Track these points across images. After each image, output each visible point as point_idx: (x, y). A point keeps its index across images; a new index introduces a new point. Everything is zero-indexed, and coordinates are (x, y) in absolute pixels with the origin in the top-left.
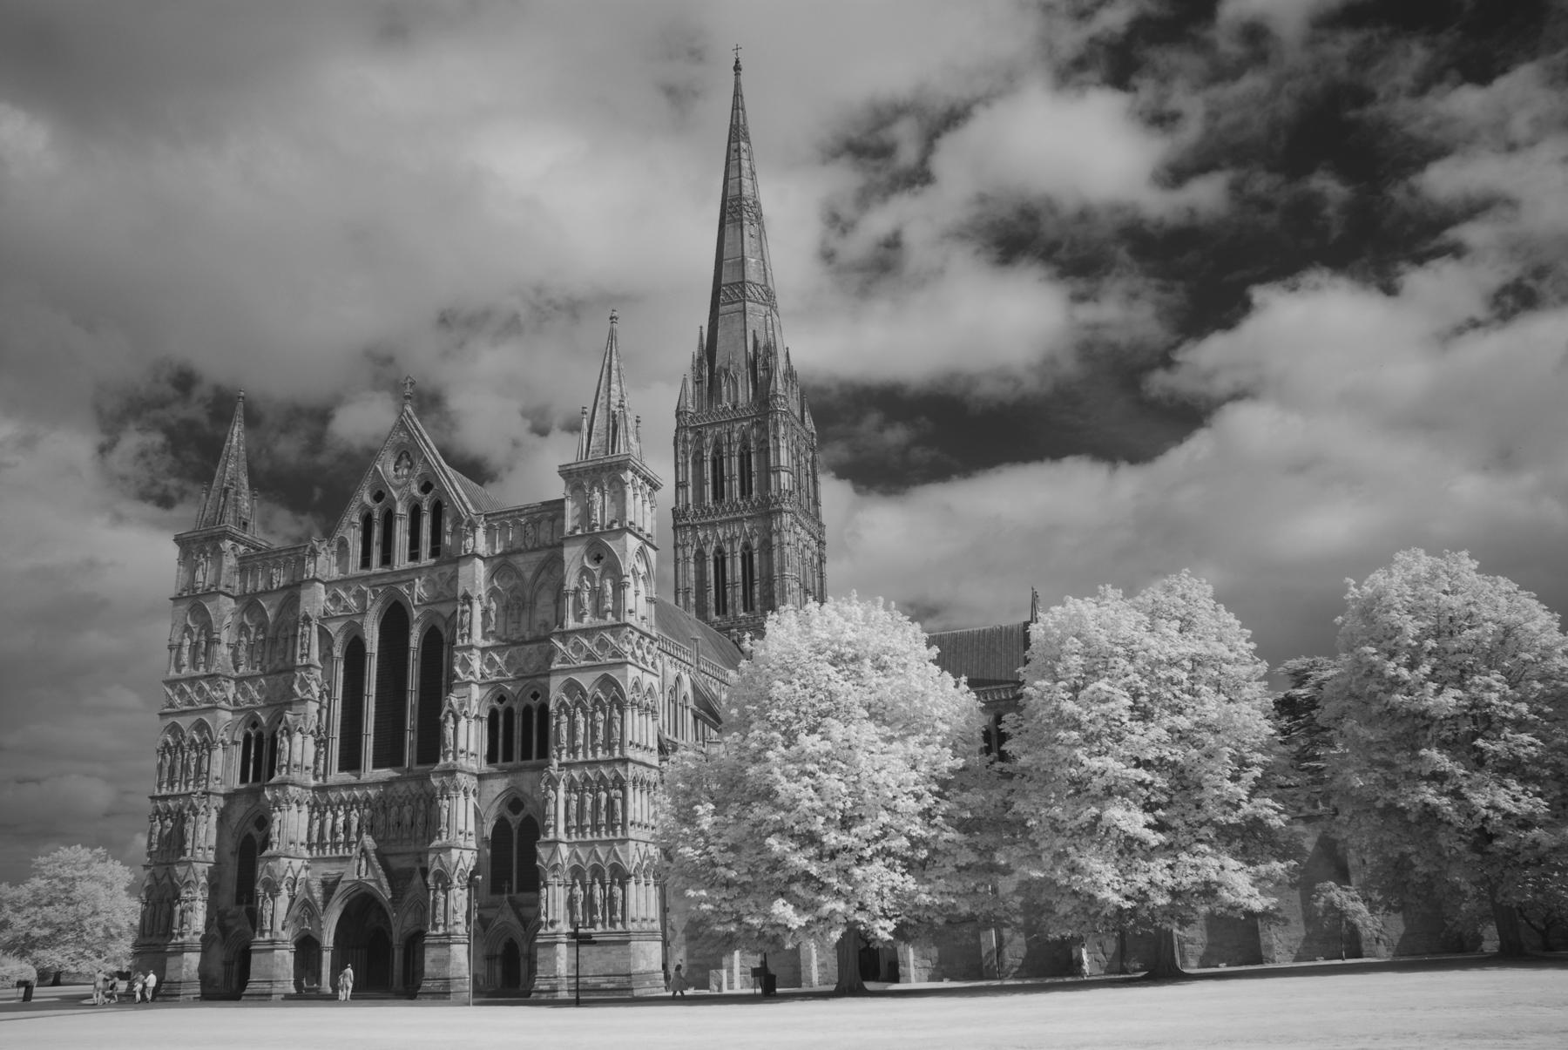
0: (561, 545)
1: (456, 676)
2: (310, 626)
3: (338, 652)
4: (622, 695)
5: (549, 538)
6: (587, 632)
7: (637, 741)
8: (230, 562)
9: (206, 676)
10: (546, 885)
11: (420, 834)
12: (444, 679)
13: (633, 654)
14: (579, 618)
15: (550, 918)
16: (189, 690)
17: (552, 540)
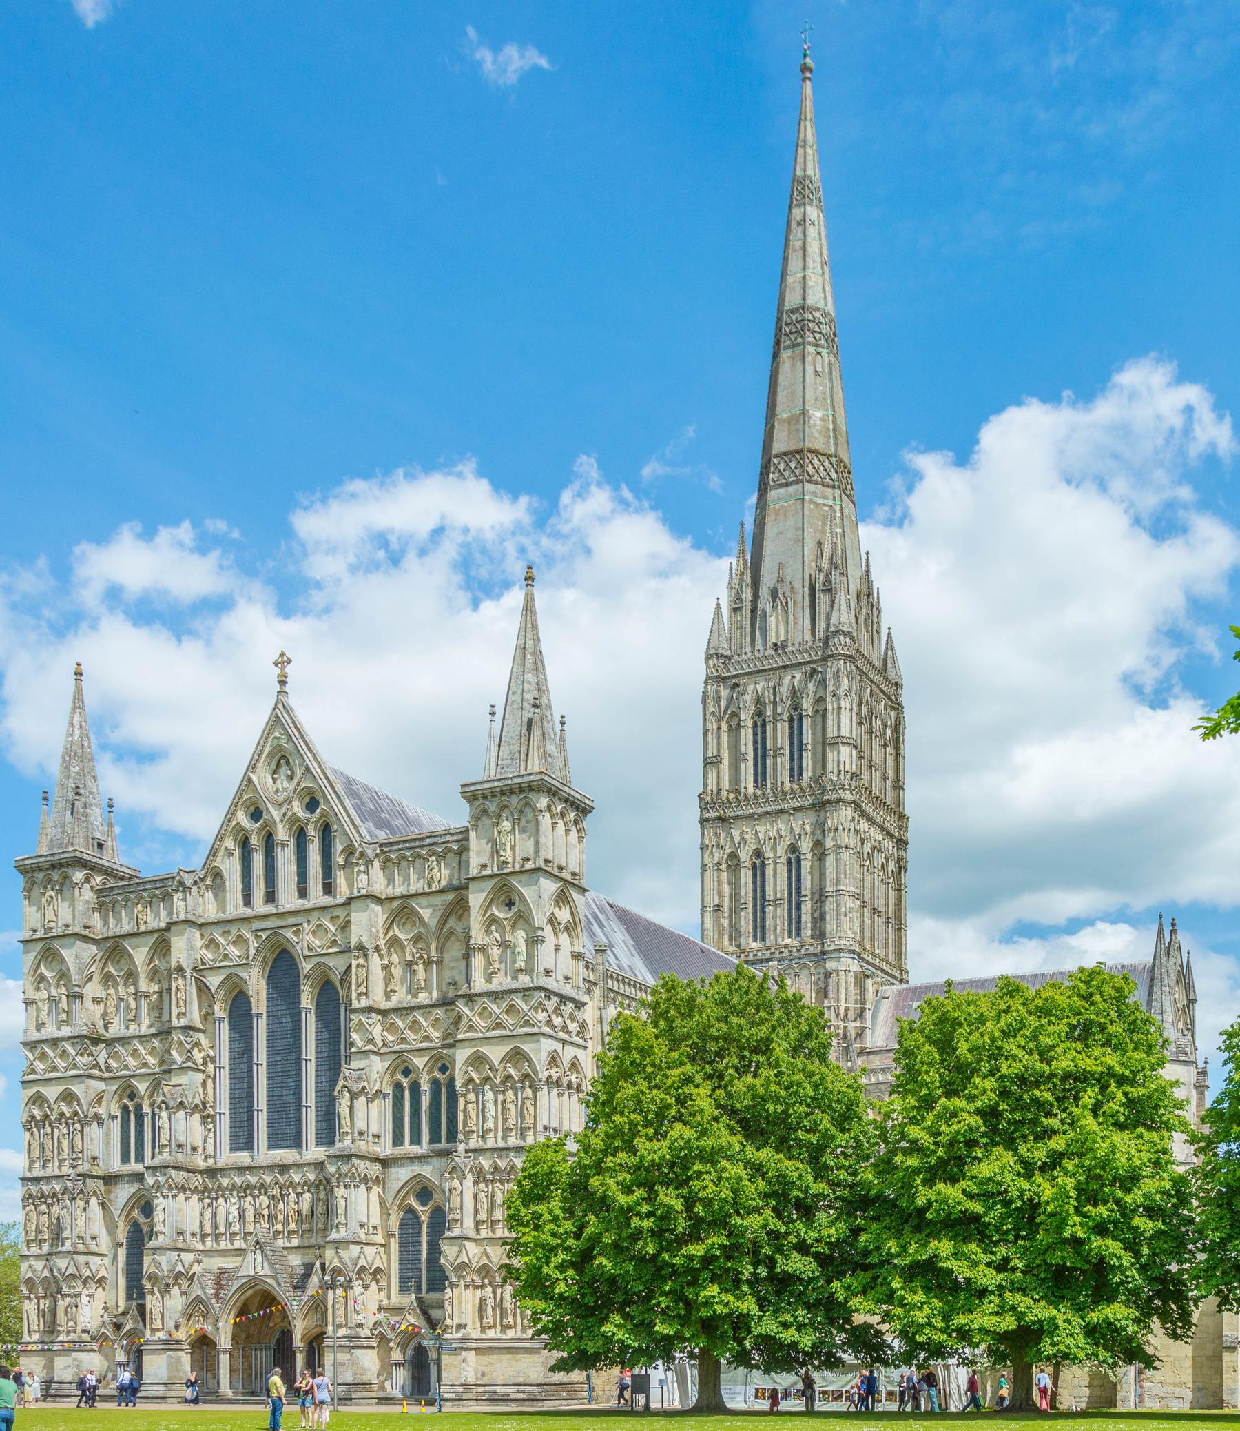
0: (466, 887)
1: (352, 1044)
2: (184, 977)
3: (220, 1010)
4: (536, 1074)
5: (456, 876)
6: (496, 996)
7: (554, 1124)
8: (88, 895)
9: (70, 1038)
10: (452, 1286)
11: (321, 1225)
12: (342, 1046)
13: (549, 1023)
14: (489, 977)
15: (456, 1321)
16: (50, 1053)
17: (459, 879)
